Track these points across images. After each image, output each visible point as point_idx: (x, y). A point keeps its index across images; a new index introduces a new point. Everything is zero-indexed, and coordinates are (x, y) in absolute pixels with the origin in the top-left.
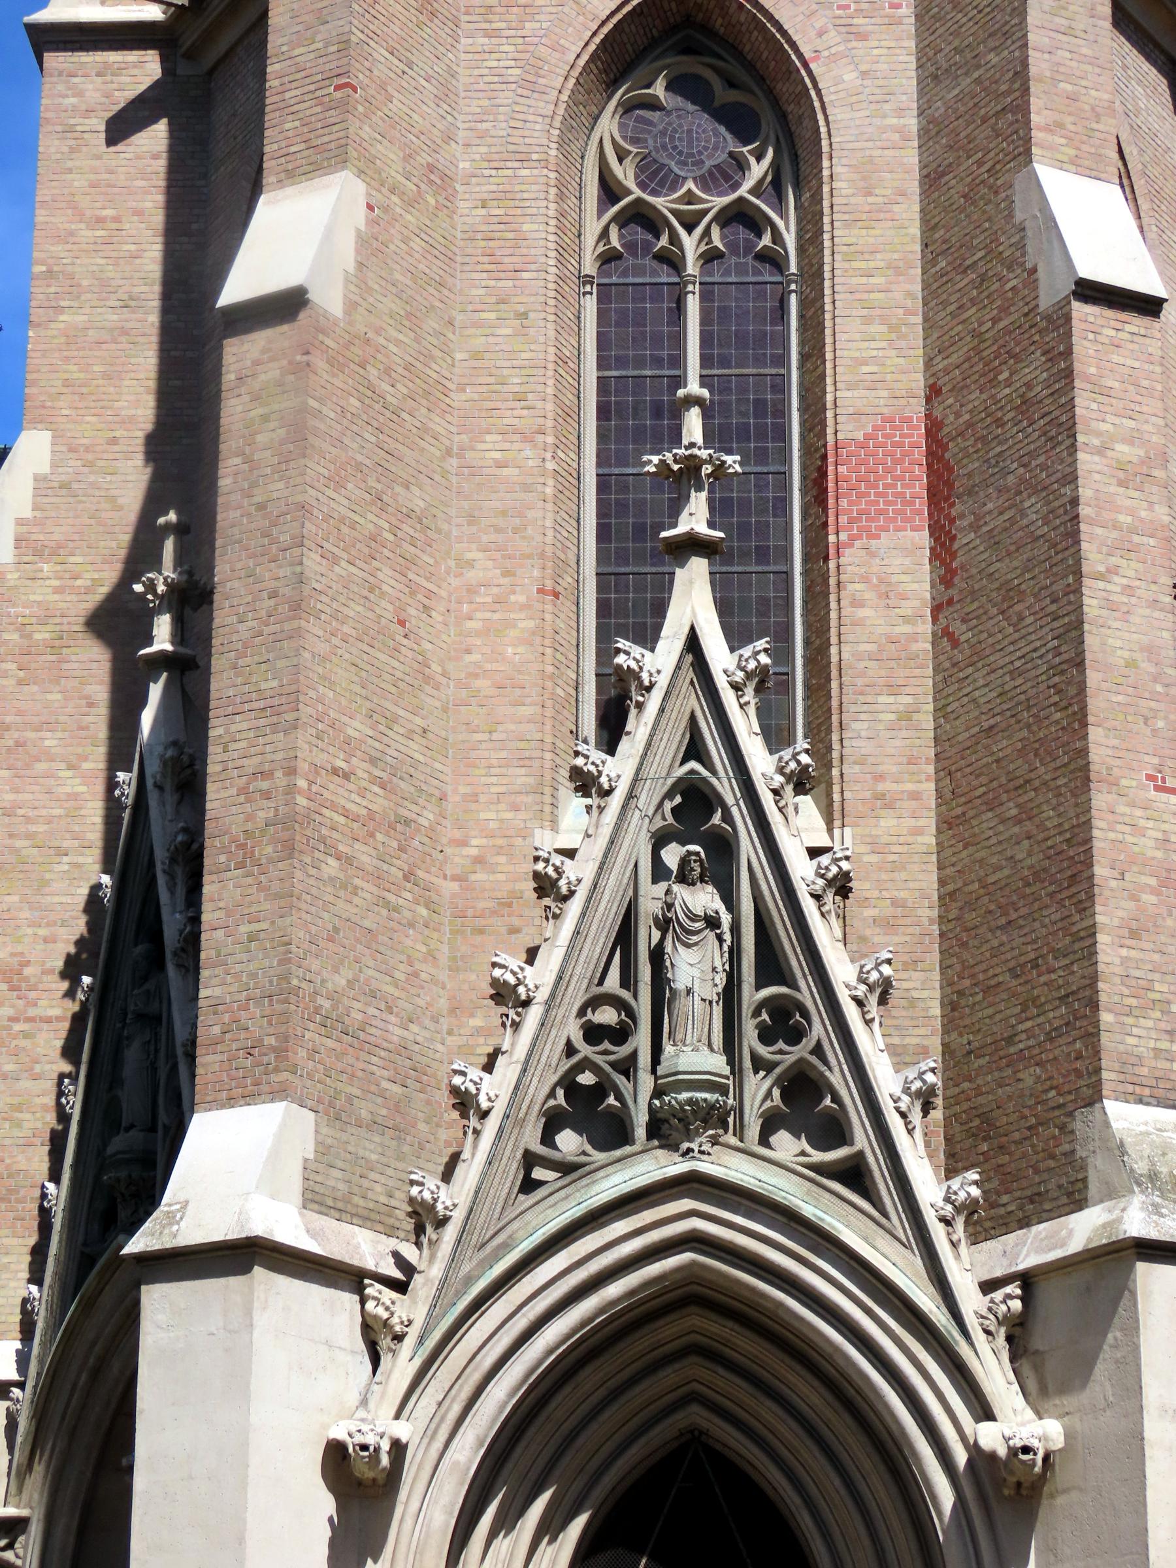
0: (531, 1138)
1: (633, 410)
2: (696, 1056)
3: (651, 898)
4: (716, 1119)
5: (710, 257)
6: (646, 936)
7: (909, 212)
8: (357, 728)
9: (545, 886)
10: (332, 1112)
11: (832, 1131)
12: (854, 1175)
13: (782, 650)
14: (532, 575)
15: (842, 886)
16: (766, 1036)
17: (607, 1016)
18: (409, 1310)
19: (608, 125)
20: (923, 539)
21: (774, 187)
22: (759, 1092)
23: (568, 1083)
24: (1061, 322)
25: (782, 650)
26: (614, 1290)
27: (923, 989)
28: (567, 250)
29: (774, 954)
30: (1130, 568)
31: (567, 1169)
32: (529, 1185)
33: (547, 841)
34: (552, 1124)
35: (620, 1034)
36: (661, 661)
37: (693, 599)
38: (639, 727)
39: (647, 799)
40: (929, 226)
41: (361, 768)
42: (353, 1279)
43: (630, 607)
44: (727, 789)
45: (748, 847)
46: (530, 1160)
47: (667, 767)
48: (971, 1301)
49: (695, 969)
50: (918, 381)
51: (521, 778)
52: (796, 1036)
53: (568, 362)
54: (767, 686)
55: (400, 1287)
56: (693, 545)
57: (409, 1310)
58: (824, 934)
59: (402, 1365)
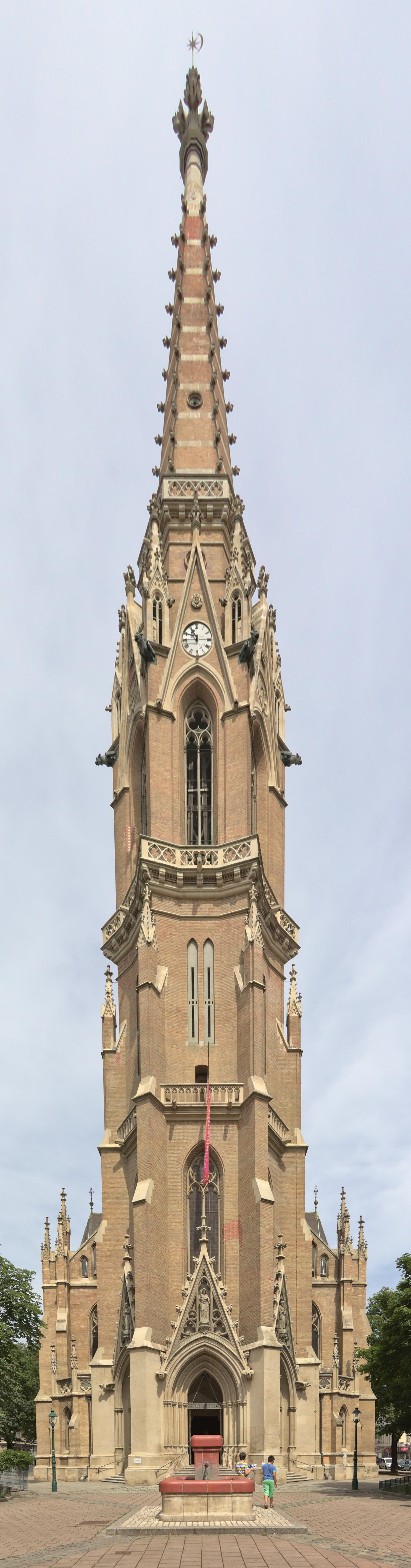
1: (196, 1219)
3: (198, 1297)
4: (208, 1329)
5: (206, 1193)
6: (198, 1303)
7: (237, 1185)
9: (183, 1295)
10: (155, 1328)
11: (224, 1330)
12: (226, 1336)
13: (217, 1258)
14: (180, 1246)
15: (225, 1294)
17: (193, 1314)
18: (166, 1356)
19: (190, 1169)
20: (238, 1240)
21: (216, 1180)
22: (213, 1325)
23: (188, 1324)
24: (259, 1205)
25: (217, 1258)
27: (237, 1310)
28: (185, 1192)
30: (267, 1246)
32: (182, 1338)
33: (183, 1288)
34: (185, 1330)
37: (204, 1250)
38: (196, 1270)
39: (198, 1282)
40: (240, 1188)
42: (158, 1351)
44: (209, 1280)
45: (212, 1288)
46: (182, 1335)
47: (201, 1277)
48: (242, 1354)
49: (205, 1307)
50: (237, 1214)
51: (180, 1278)
53: (185, 1210)
54: (215, 1264)
56: (204, 1241)
57: (166, 1356)
58: (223, 1302)
59: (165, 1364)
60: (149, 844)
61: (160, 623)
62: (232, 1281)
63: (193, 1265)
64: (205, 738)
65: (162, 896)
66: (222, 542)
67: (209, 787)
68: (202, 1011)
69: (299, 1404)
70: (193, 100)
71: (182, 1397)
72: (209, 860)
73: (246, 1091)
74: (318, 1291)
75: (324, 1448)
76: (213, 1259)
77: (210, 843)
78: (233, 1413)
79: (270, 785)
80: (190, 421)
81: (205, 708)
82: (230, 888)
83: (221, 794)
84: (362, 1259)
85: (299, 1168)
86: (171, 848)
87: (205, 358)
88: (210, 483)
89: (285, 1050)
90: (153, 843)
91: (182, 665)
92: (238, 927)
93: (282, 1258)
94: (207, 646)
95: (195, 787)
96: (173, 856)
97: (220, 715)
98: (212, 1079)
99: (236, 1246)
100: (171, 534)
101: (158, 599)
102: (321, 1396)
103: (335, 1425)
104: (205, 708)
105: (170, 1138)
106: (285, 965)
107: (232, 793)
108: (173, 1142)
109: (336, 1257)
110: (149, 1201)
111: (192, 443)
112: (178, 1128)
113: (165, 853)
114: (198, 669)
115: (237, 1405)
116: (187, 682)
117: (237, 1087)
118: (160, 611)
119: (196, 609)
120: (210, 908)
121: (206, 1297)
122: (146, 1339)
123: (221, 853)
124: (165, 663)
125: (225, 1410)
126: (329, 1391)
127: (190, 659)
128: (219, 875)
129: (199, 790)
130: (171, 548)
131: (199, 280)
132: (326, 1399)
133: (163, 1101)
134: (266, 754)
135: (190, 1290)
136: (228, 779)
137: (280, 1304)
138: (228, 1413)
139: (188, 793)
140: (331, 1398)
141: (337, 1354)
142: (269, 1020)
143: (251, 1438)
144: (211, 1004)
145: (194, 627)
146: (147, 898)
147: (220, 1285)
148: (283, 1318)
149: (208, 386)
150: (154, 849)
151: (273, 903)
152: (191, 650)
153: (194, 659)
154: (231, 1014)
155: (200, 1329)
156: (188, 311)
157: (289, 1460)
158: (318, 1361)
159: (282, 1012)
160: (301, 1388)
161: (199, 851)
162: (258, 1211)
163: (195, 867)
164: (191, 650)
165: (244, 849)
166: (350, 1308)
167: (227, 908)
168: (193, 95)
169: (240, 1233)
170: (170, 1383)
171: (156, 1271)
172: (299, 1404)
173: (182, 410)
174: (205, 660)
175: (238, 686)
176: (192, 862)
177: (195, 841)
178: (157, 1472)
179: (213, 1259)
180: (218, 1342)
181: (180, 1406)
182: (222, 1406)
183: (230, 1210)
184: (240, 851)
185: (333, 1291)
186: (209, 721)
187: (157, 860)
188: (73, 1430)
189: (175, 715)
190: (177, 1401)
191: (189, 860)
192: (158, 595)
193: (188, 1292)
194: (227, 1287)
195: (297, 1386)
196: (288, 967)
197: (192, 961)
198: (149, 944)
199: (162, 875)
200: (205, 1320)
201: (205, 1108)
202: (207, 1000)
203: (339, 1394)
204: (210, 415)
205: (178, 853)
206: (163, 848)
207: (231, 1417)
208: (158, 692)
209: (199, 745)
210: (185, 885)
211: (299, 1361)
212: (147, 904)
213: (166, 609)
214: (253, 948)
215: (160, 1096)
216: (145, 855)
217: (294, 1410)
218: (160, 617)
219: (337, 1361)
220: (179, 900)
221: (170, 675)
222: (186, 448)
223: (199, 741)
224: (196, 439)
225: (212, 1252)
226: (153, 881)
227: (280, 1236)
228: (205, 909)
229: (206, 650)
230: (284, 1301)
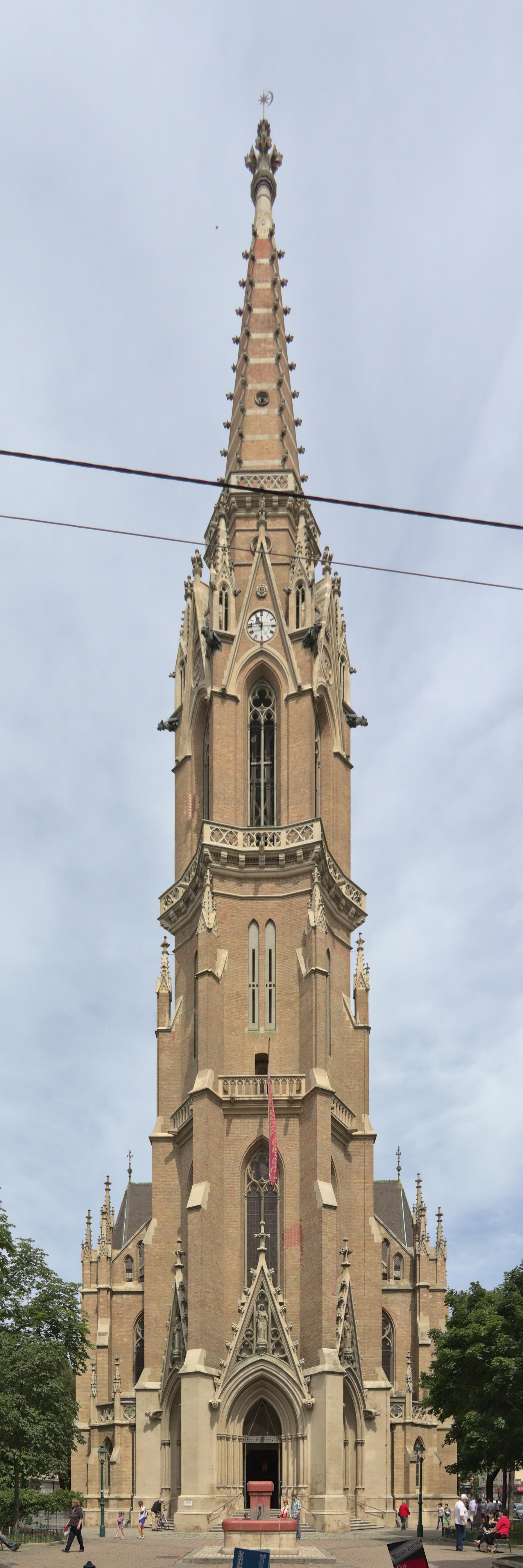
0: (238, 1353)
2: (262, 1340)
3: (256, 1314)
4: (265, 1350)
6: (255, 1320)
8: (210, 1284)
9: (240, 1311)
10: (208, 1350)
11: (283, 1352)
12: (286, 1359)
13: (276, 1271)
15: (285, 1311)
16: (273, 1336)
17: (249, 1333)
18: (220, 1381)
22: (272, 1346)
23: (244, 1344)
25: (276, 1271)
26: (250, 1378)
27: (297, 1327)
29: (274, 1321)
31: (243, 1358)
32: (238, 1361)
34: (241, 1351)
35: (251, 1336)
36: (257, 1272)
37: (262, 1261)
38: (254, 1284)
39: (255, 1296)
41: (211, 1291)
42: (212, 1376)
43: (253, 1263)
44: (267, 1294)
45: (270, 1304)
46: (238, 1357)
48: (303, 1380)
49: (262, 1325)
52: (277, 1336)
54: (274, 1276)
55: (219, 1377)
56: (262, 1251)
57: (220, 1381)
58: (282, 1319)
59: (219, 1390)
60: (212, 828)
61: (226, 611)
62: (292, 1294)
63: (250, 1277)
64: (269, 715)
65: (223, 877)
66: (287, 527)
67: (272, 759)
68: (263, 995)
69: (368, 1436)
70: (263, 146)
71: (236, 1428)
72: (272, 841)
73: (308, 1083)
74: (391, 1297)
75: (396, 1489)
76: (272, 1271)
77: (273, 824)
78: (292, 1448)
79: (335, 750)
80: (258, 417)
81: (269, 686)
82: (293, 868)
83: (284, 773)
84: (440, 1259)
85: (367, 1159)
86: (233, 831)
87: (273, 360)
88: (275, 477)
89: (352, 1027)
90: (216, 827)
91: (246, 650)
92: (301, 908)
93: (347, 1266)
94: (272, 632)
95: (259, 760)
96: (235, 838)
97: (284, 696)
98: (273, 1070)
99: (298, 1255)
100: (238, 521)
101: (224, 589)
102: (393, 1426)
103: (408, 1461)
104: (269, 686)
105: (228, 1133)
106: (352, 934)
107: (295, 773)
108: (231, 1137)
109: (411, 1257)
110: (204, 1207)
111: (258, 437)
112: (236, 1122)
113: (227, 836)
114: (262, 653)
115: (297, 1439)
116: (252, 665)
117: (299, 1078)
118: (226, 600)
120: (272, 888)
121: (263, 1313)
122: (199, 1363)
123: (283, 835)
124: (230, 648)
125: (284, 1444)
126: (401, 1420)
127: (254, 645)
128: (282, 856)
129: (262, 763)
130: (237, 534)
131: (267, 293)
132: (399, 1428)
133: (220, 1094)
134: (332, 725)
135: (246, 1305)
136: (292, 759)
137: (345, 1319)
139: (251, 766)
140: (404, 1429)
141: (410, 1376)
142: (334, 996)
143: (312, 1478)
144: (272, 988)
145: (259, 614)
146: (208, 882)
147: (280, 1298)
148: (349, 1335)
149: (275, 386)
150: (216, 832)
151: (337, 875)
152: (256, 636)
153: (259, 645)
154: (293, 999)
155: (257, 1351)
156: (257, 320)
157: (356, 1504)
158: (389, 1385)
159: (349, 985)
160: (370, 1417)
161: (262, 832)
162: (320, 1217)
163: (257, 848)
164: (256, 636)
165: (307, 831)
166: (427, 1318)
167: (290, 888)
168: (263, 145)
169: (301, 1239)
170: (224, 1412)
171: (210, 1284)
172: (368, 1436)
173: (250, 408)
174: (269, 645)
175: (302, 670)
176: (255, 843)
177: (259, 823)
179: (272, 1271)
180: (276, 1366)
181: (234, 1439)
182: (281, 1440)
183: (291, 1214)
184: (303, 833)
185: (408, 1298)
186: (273, 699)
187: (219, 844)
188: (115, 1466)
189: (239, 697)
190: (231, 1433)
191: (252, 841)
192: (224, 586)
193: (245, 1308)
194: (287, 1301)
195: (365, 1415)
196: (354, 936)
197: (253, 943)
198: (209, 930)
199: (224, 858)
200: (262, 1340)
201: (267, 1101)
202: (269, 983)
203: (413, 1424)
204: (276, 411)
205: (240, 835)
206: (225, 831)
207: (290, 1452)
208: (223, 677)
209: (262, 722)
210: (246, 866)
211: (367, 1384)
212: (208, 889)
213: (232, 599)
214: (315, 933)
215: (217, 1090)
216: (207, 840)
217: (362, 1444)
218: (226, 605)
219: (411, 1385)
220: (241, 880)
221: (235, 660)
222: (253, 442)
223: (262, 718)
224: (263, 433)
225: (271, 1263)
226: (214, 864)
227: (345, 1241)
228: (267, 889)
229: (270, 635)
230: (350, 1315)
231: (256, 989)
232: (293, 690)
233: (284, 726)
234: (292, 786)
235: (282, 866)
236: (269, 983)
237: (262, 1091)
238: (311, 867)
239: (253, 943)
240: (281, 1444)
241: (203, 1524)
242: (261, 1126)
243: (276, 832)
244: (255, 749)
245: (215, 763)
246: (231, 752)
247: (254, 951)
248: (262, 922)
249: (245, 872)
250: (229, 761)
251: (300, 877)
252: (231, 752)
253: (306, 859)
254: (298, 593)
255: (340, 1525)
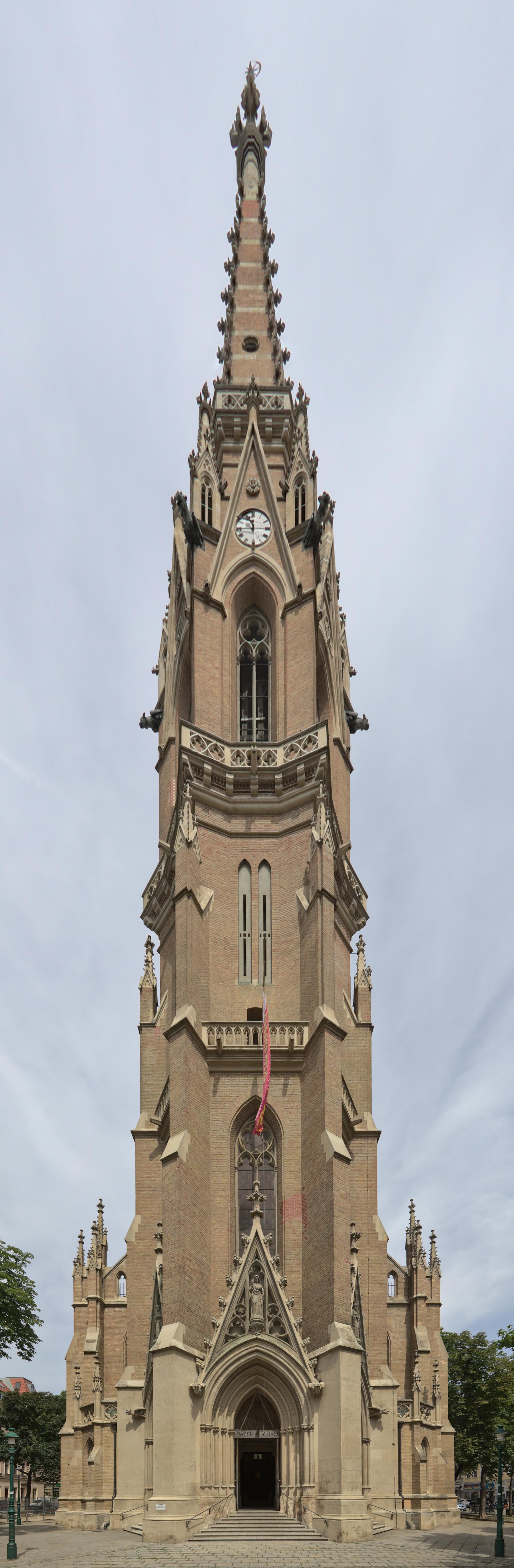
67: (266, 715)
78: (294, 1442)
81: (262, 618)
91: (234, 556)
94: (265, 536)
95: (250, 715)
104: (262, 618)
114: (253, 561)
116: (241, 577)
119: (253, 495)
125: (283, 1439)
127: (244, 549)
129: (255, 719)
138: (287, 1443)
139: (242, 723)
152: (246, 540)
174: (262, 550)
178: (188, 1523)
182: (280, 1435)
207: (292, 1448)
223: (254, 653)
229: (264, 539)
231: (248, 938)
232: (290, 597)
233: (280, 664)
234: (290, 709)
235: (279, 794)
236: (263, 933)
237: (256, 1041)
238: (313, 791)
239: (244, 887)
240: (280, 1439)
241: (180, 1532)
242: (255, 1085)
243: (271, 749)
244: (245, 706)
245: (196, 675)
246: (217, 668)
247: (245, 896)
248: (255, 863)
249: (235, 802)
250: (214, 678)
251: (301, 809)
252: (217, 668)
253: (308, 779)
254: (297, 493)
255: (361, 1533)
